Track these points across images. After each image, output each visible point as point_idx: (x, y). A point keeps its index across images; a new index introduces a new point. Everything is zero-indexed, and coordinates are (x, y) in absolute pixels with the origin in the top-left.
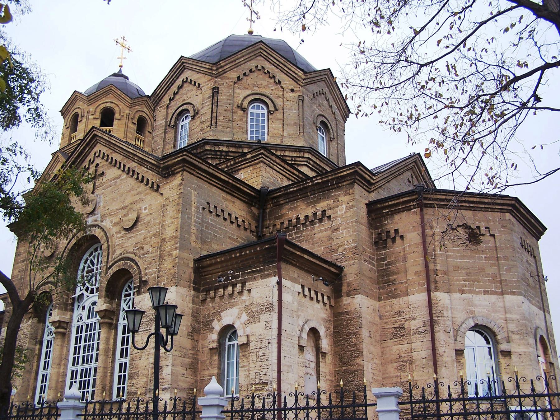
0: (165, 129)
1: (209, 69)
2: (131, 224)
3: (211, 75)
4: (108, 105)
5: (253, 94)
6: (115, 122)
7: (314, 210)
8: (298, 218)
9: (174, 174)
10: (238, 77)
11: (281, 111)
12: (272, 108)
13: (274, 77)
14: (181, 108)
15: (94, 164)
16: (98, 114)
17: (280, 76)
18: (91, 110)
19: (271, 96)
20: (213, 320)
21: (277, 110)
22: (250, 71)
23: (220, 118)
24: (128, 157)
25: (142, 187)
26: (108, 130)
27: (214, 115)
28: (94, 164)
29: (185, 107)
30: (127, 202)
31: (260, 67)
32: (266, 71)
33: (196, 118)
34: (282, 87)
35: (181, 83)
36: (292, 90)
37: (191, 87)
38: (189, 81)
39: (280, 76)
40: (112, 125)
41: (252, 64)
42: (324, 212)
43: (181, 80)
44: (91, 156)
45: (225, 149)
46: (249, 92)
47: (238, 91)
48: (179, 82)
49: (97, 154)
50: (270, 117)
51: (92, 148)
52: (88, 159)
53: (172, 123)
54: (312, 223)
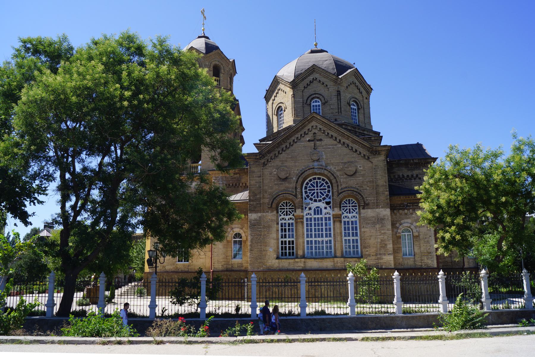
4: (217, 63)
6: (221, 75)
7: (411, 173)
8: (403, 175)
9: (379, 154)
13: (359, 89)
14: (315, 96)
15: (312, 132)
17: (362, 89)
20: (396, 224)
23: (342, 109)
24: (344, 137)
25: (355, 155)
27: (339, 107)
28: (312, 132)
29: (317, 95)
30: (345, 161)
33: (326, 104)
37: (319, 84)
39: (362, 89)
42: (417, 176)
44: (309, 127)
46: (351, 95)
48: (311, 78)
51: (309, 123)
52: (307, 128)
54: (411, 179)
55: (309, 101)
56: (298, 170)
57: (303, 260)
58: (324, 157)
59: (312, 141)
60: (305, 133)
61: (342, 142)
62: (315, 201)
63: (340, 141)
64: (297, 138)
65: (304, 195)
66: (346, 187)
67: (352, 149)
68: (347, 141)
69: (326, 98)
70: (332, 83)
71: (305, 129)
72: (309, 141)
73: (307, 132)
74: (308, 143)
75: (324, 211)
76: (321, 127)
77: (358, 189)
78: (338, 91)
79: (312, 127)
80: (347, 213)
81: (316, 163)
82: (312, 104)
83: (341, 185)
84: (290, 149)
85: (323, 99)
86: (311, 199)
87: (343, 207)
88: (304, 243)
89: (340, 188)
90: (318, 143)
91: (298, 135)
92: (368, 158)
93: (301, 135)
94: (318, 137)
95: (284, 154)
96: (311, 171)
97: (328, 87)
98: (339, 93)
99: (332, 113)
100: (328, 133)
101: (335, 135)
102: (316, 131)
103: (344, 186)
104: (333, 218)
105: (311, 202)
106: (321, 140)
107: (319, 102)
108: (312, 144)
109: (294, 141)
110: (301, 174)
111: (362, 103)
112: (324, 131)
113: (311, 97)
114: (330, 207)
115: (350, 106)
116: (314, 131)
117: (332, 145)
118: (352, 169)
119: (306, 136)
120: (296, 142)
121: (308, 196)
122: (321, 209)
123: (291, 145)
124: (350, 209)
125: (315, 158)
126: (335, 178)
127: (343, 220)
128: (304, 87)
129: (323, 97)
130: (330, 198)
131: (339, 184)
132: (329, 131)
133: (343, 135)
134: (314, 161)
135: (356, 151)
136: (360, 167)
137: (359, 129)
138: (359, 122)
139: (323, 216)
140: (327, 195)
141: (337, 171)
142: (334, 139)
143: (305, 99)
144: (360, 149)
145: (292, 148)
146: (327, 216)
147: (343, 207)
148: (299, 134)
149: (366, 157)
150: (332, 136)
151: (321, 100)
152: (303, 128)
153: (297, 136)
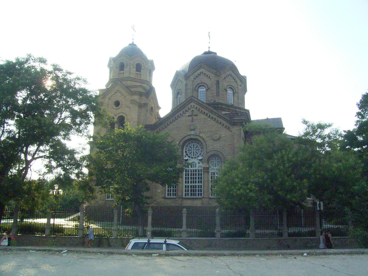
0: (193, 91)
1: (215, 72)
2: (217, 138)
3: (216, 75)
5: (229, 85)
6: (142, 71)
10: (225, 78)
11: (237, 93)
12: (235, 92)
13: (235, 79)
14: (201, 84)
16: (135, 66)
18: (132, 63)
19: (235, 87)
21: (236, 92)
22: (228, 75)
23: (220, 94)
25: (220, 126)
26: (138, 74)
28: (191, 110)
29: (202, 84)
31: (231, 75)
32: (232, 76)
33: (209, 90)
34: (237, 84)
35: (199, 73)
36: (240, 86)
38: (204, 73)
39: (237, 79)
40: (140, 72)
41: (228, 73)
43: (200, 72)
44: (189, 106)
45: (224, 107)
46: (227, 84)
47: (225, 83)
48: (199, 72)
49: (193, 107)
50: (234, 95)
51: (189, 103)
52: (187, 107)
53: (196, 89)
55: (197, 88)
56: (180, 136)
57: (181, 199)
58: (199, 128)
59: (191, 116)
60: (186, 111)
61: (211, 117)
62: (192, 158)
63: (210, 116)
64: (181, 114)
65: (185, 154)
66: (212, 149)
67: (218, 122)
68: (214, 116)
69: (209, 85)
70: (213, 75)
71: (186, 108)
72: (189, 116)
73: (187, 110)
74: (188, 117)
75: (198, 165)
76: (197, 106)
77: (220, 150)
78: (217, 81)
79: (191, 106)
80: (213, 166)
81: (192, 133)
82: (199, 90)
83: (209, 147)
84: (175, 122)
85: (206, 86)
86: (189, 157)
87: (211, 162)
88: (183, 187)
89: (208, 148)
90: (194, 117)
91: (181, 112)
92: (229, 128)
93: (183, 112)
94: (195, 114)
95: (171, 125)
96: (188, 138)
97: (211, 78)
98: (218, 83)
99: (212, 97)
100: (202, 111)
101: (206, 112)
102: (194, 109)
103: (211, 148)
104: (203, 170)
105: (189, 158)
106: (197, 115)
107: (204, 89)
108: (190, 118)
109: (178, 116)
110: (182, 139)
111: (236, 89)
112: (199, 109)
113: (200, 86)
114: (202, 162)
115: (227, 91)
116: (192, 109)
117: (204, 119)
118: (218, 136)
119: (186, 113)
120: (180, 117)
121: (187, 155)
122: (196, 163)
123: (176, 119)
124: (215, 164)
125: (192, 128)
126: (205, 142)
127: (210, 171)
128: (194, 78)
129: (207, 85)
130: (202, 156)
131: (208, 146)
132: (202, 109)
133: (212, 112)
134: (191, 130)
135: (221, 123)
136: (223, 134)
137: (232, 107)
138: (233, 102)
139: (197, 168)
140: (200, 154)
141: (207, 137)
142: (206, 114)
143: (194, 87)
144: (223, 122)
145: (177, 121)
146: (200, 168)
147: (211, 162)
148: (182, 111)
149: (228, 128)
150: (204, 112)
151: (205, 87)
152: (184, 107)
153: (180, 113)
